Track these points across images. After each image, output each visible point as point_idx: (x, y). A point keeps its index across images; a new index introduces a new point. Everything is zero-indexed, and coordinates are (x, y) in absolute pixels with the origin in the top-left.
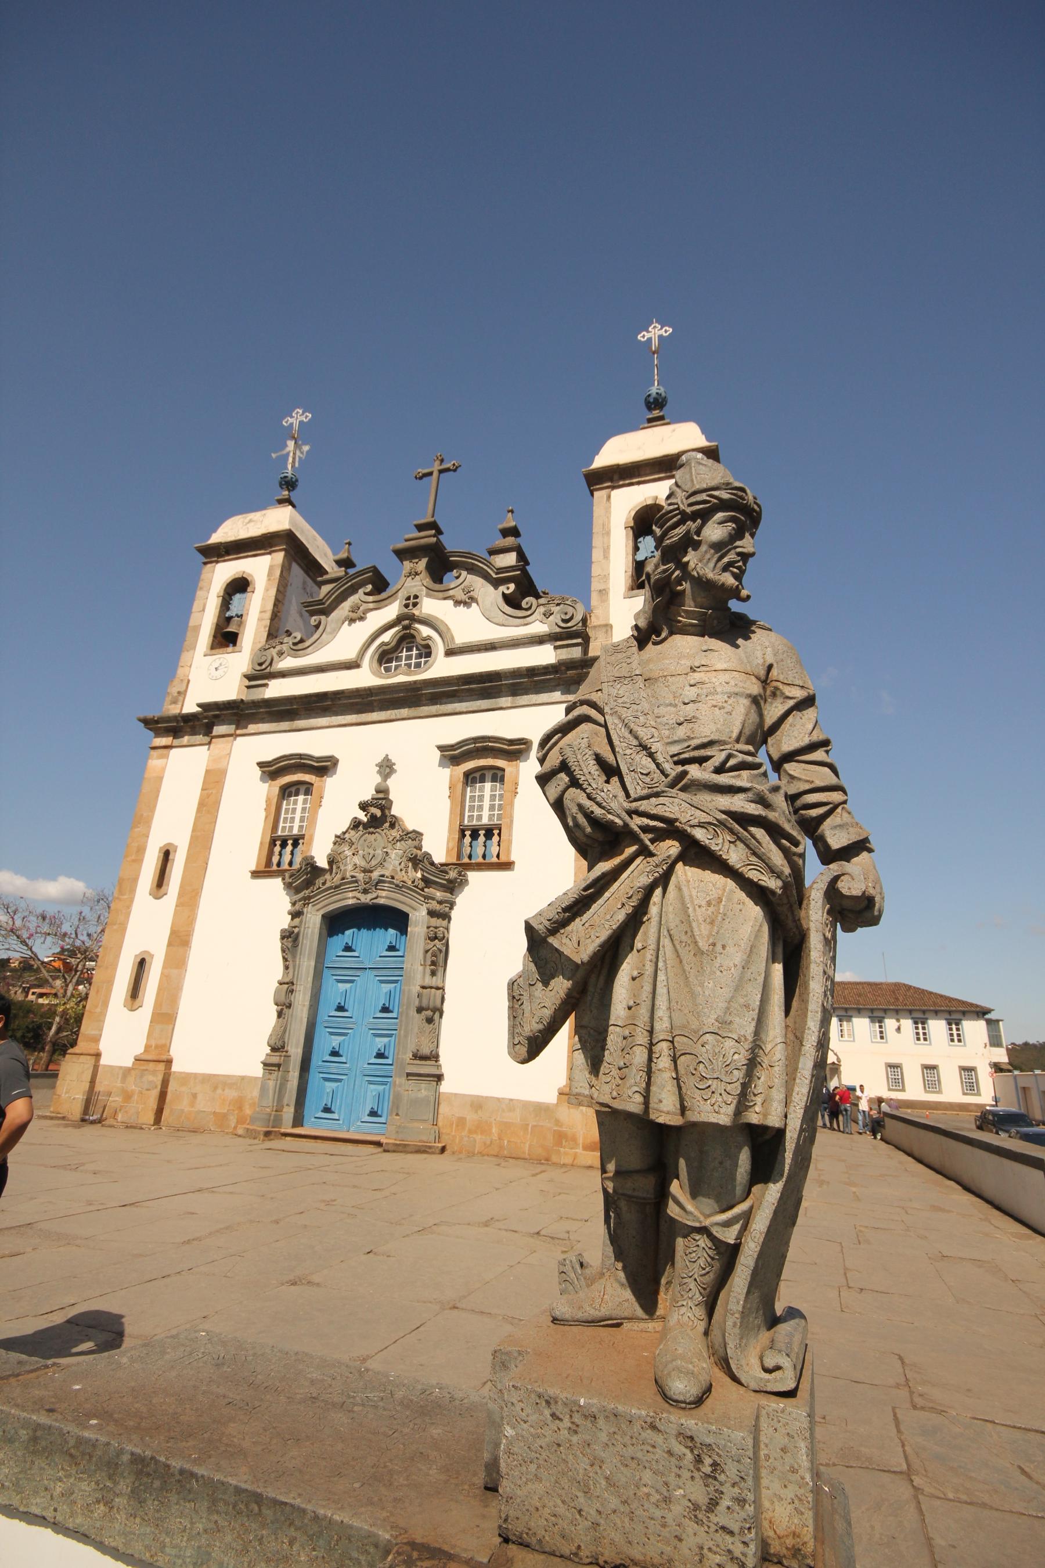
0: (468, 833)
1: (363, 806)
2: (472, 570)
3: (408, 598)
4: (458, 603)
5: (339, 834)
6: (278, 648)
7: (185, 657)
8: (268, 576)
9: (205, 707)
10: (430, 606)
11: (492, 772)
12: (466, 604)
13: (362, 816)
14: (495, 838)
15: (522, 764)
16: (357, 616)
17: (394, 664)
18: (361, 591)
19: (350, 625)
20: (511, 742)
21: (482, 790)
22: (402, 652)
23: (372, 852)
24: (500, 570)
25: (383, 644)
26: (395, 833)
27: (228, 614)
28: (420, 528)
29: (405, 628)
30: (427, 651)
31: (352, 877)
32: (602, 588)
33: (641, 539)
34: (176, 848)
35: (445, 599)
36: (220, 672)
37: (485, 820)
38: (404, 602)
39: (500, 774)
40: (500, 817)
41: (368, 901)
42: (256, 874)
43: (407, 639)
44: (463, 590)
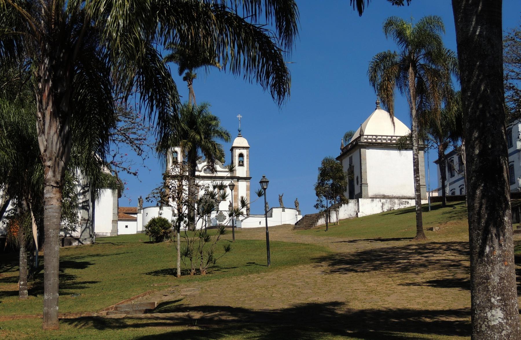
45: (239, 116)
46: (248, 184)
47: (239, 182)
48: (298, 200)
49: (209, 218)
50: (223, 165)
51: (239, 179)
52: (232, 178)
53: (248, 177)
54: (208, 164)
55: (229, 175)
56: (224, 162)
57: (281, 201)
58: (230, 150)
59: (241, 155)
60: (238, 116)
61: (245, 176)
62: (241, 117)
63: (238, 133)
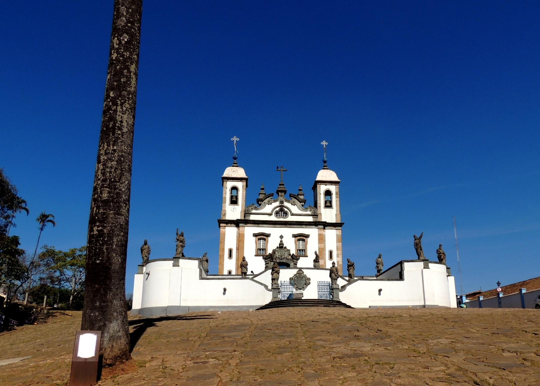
0: (299, 250)
1: (280, 245)
2: (295, 198)
3: (281, 201)
4: (292, 205)
5: (274, 249)
6: (251, 207)
7: (223, 204)
8: (243, 188)
9: (238, 220)
10: (286, 204)
12: (294, 205)
14: (304, 252)
15: (308, 239)
16: (269, 203)
17: (278, 215)
18: (270, 198)
19: (268, 205)
20: (307, 235)
21: (300, 242)
24: (302, 200)
25: (277, 211)
26: (286, 249)
27: (232, 195)
28: (280, 185)
29: (282, 208)
30: (286, 214)
32: (320, 206)
34: (232, 249)
35: (289, 203)
36: (234, 210)
37: (301, 248)
40: (304, 248)
42: (256, 256)
43: (282, 210)
45: (324, 143)
46: (339, 232)
47: (326, 230)
48: (442, 248)
49: (275, 282)
50: (303, 206)
51: (326, 225)
52: (315, 224)
53: (338, 222)
54: (280, 205)
55: (310, 219)
56: (305, 202)
57: (420, 247)
58: (313, 189)
59: (328, 193)
60: (322, 143)
61: (334, 221)
62: (327, 144)
63: (323, 164)
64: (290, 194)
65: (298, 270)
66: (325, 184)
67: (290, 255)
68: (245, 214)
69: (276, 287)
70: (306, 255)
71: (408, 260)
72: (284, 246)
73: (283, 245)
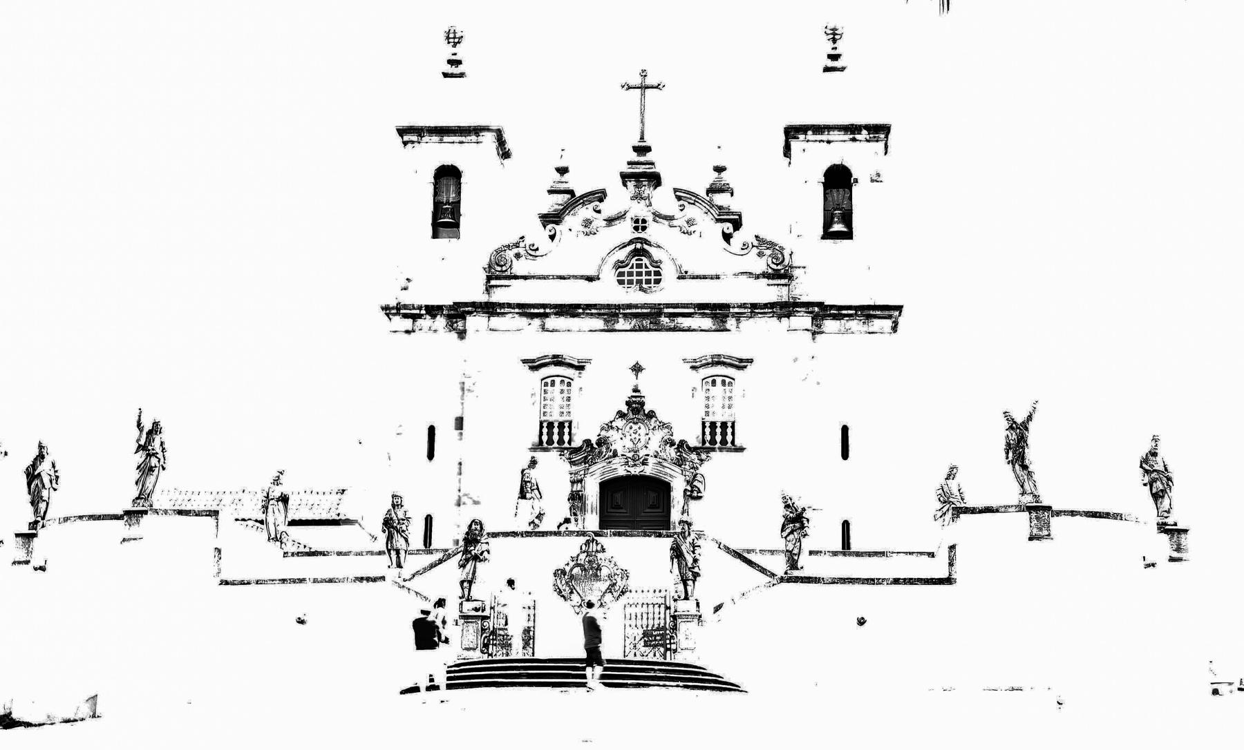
0: (708, 424)
1: (628, 403)
3: (637, 221)
6: (515, 251)
11: (721, 378)
13: (624, 409)
18: (591, 206)
20: (741, 360)
22: (632, 267)
23: (638, 438)
31: (622, 455)
33: (828, 191)
38: (634, 225)
39: (728, 380)
41: (637, 473)
44: (688, 222)
50: (727, 237)
54: (637, 235)
56: (737, 225)
64: (676, 190)
65: (583, 540)
66: (825, 137)
67: (672, 444)
68: (489, 279)
69: (474, 613)
70: (737, 443)
71: (974, 508)
72: (647, 408)
73: (642, 404)
